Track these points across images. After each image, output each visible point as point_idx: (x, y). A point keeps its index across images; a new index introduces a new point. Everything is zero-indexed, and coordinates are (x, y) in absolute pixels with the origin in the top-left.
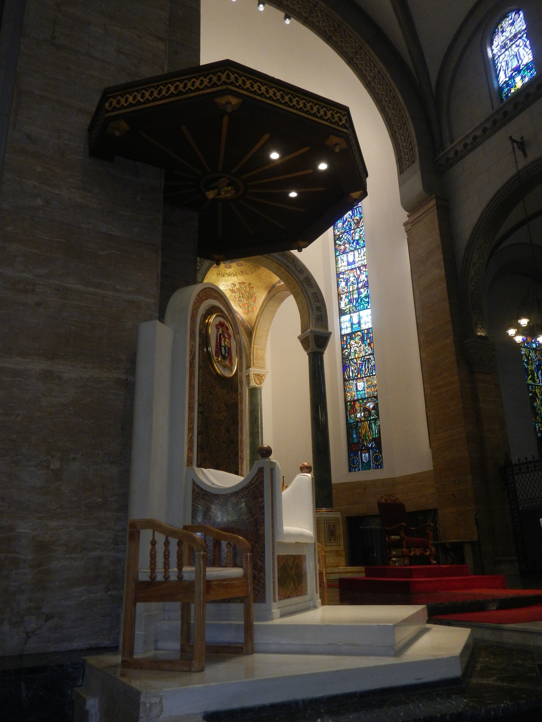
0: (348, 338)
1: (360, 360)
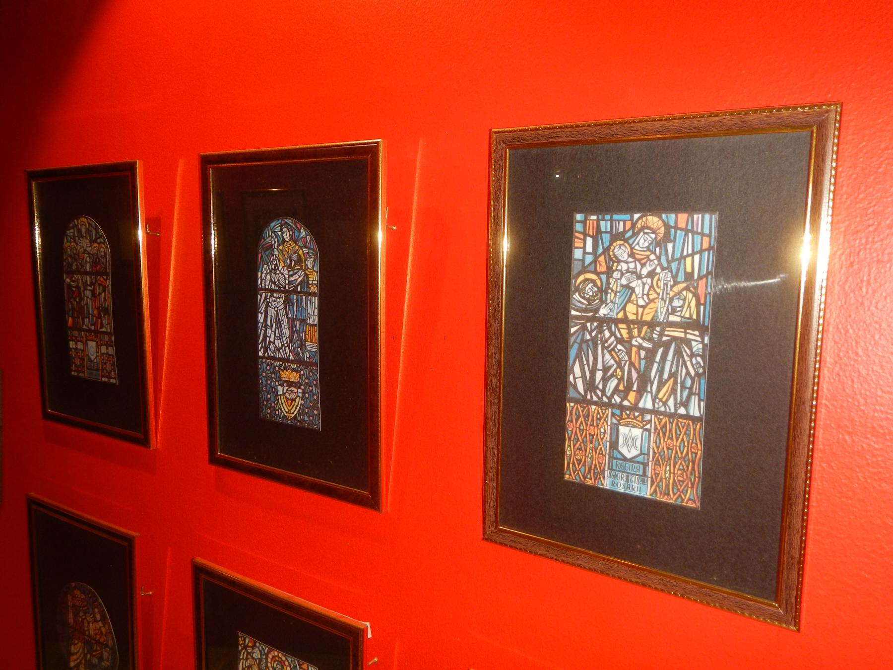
0: (603, 229)
1: (642, 336)
